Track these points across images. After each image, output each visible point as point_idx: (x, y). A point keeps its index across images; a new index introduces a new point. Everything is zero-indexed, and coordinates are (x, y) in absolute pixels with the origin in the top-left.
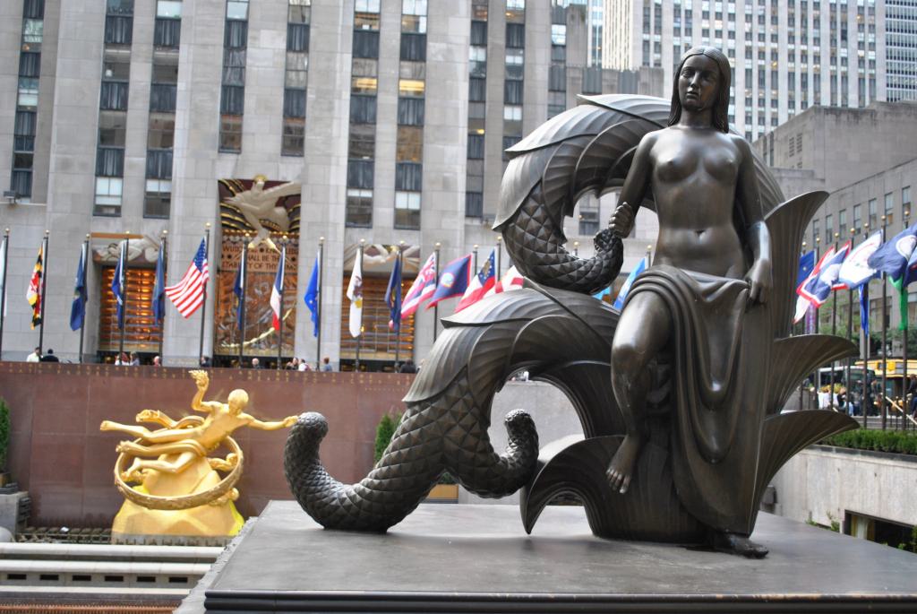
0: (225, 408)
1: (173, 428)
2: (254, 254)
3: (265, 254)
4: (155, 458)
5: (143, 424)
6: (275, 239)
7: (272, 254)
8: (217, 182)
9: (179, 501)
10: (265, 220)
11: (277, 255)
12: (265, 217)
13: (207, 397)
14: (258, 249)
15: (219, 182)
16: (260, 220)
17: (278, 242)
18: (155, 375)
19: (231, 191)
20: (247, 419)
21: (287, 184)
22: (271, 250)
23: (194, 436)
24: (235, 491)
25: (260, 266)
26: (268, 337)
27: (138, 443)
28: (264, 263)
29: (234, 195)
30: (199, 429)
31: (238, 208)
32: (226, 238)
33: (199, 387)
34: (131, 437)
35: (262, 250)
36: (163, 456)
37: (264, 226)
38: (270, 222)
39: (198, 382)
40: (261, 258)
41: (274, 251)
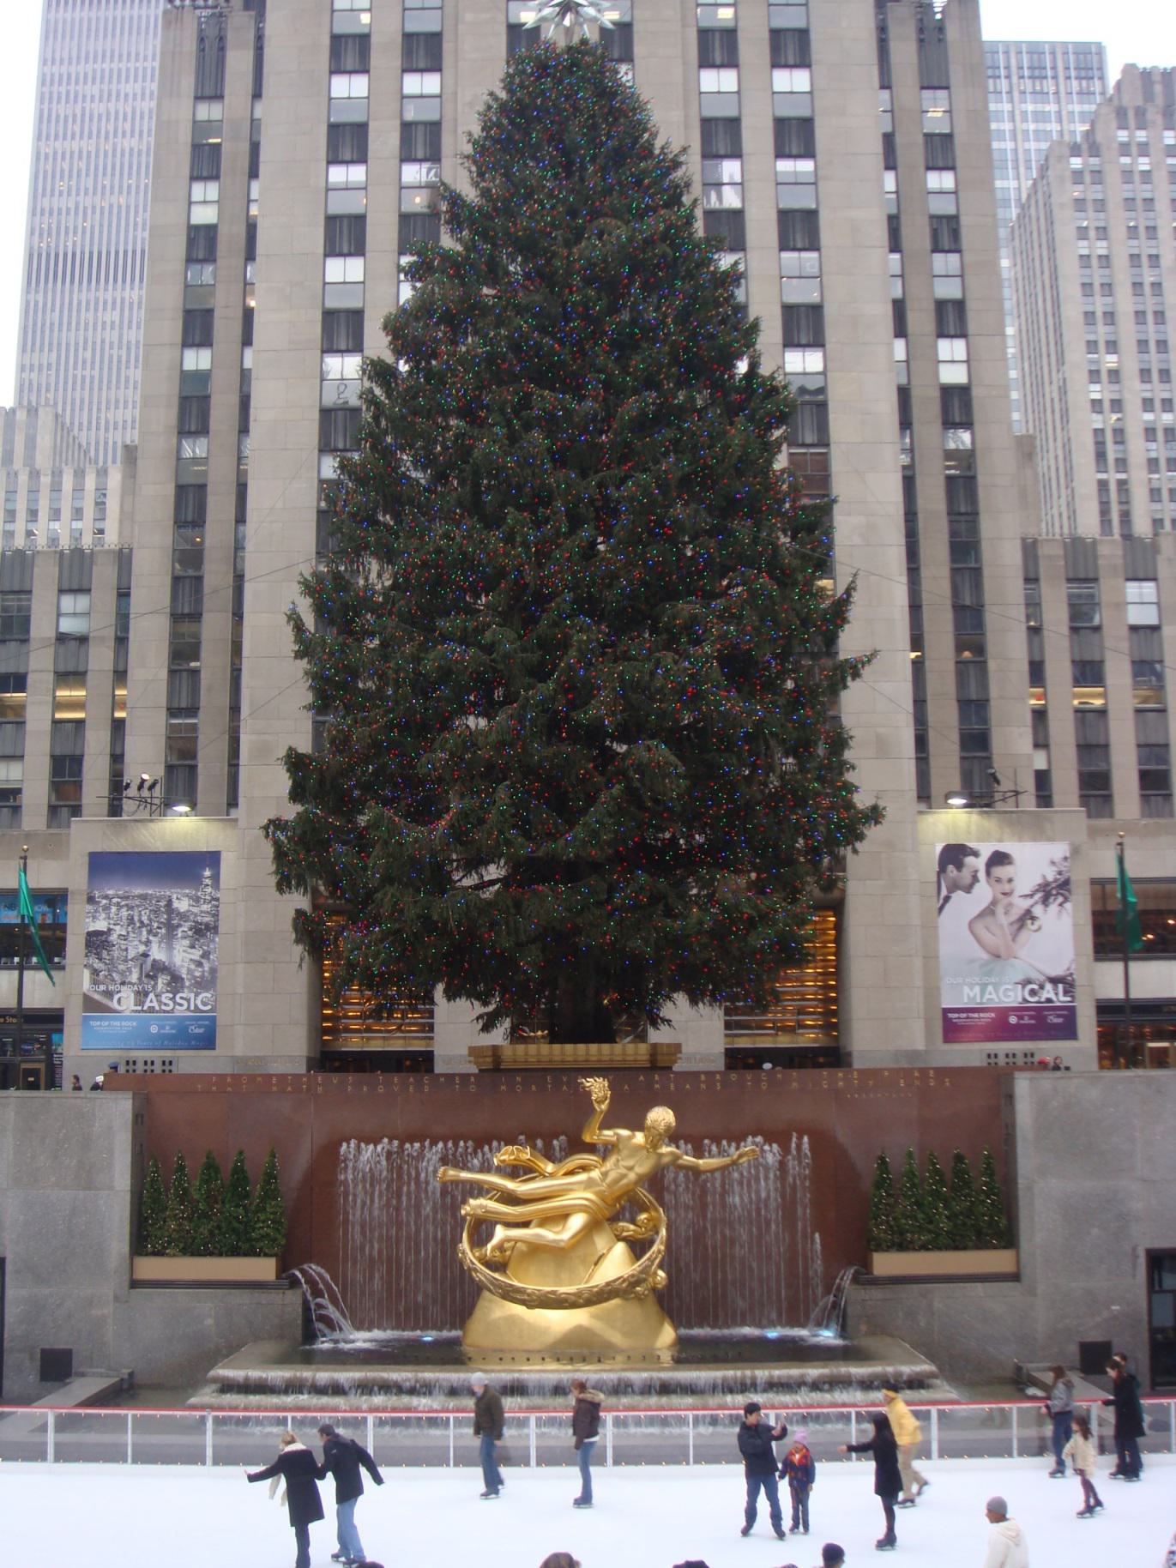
0: (640, 1138)
1: (552, 1175)
4: (526, 1225)
5: (502, 1171)
9: (579, 1294)
13: (606, 1125)
18: (503, 1087)
20: (671, 1153)
23: (589, 1184)
24: (661, 1273)
27: (490, 1199)
30: (595, 1174)
33: (596, 1105)
34: (478, 1190)
36: (533, 1224)
39: (594, 1097)
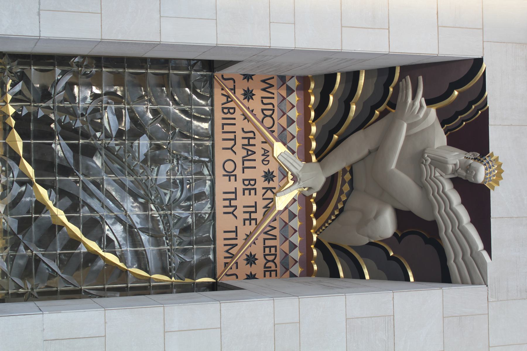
2: (258, 156)
3: (261, 184)
6: (296, 209)
7: (262, 204)
8: (477, 55)
10: (351, 183)
11: (259, 216)
12: (360, 182)
14: (273, 167)
15: (478, 62)
16: (351, 172)
17: (292, 216)
19: (449, 93)
21: (480, 245)
22: (273, 200)
25: (230, 175)
26: (40, 207)
28: (240, 187)
29: (429, 102)
31: (383, 114)
32: (294, 83)
35: (269, 176)
37: (332, 181)
38: (348, 195)
40: (249, 174)
41: (269, 208)
